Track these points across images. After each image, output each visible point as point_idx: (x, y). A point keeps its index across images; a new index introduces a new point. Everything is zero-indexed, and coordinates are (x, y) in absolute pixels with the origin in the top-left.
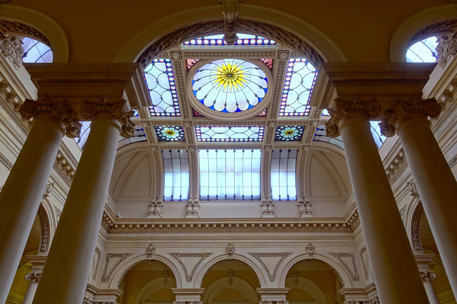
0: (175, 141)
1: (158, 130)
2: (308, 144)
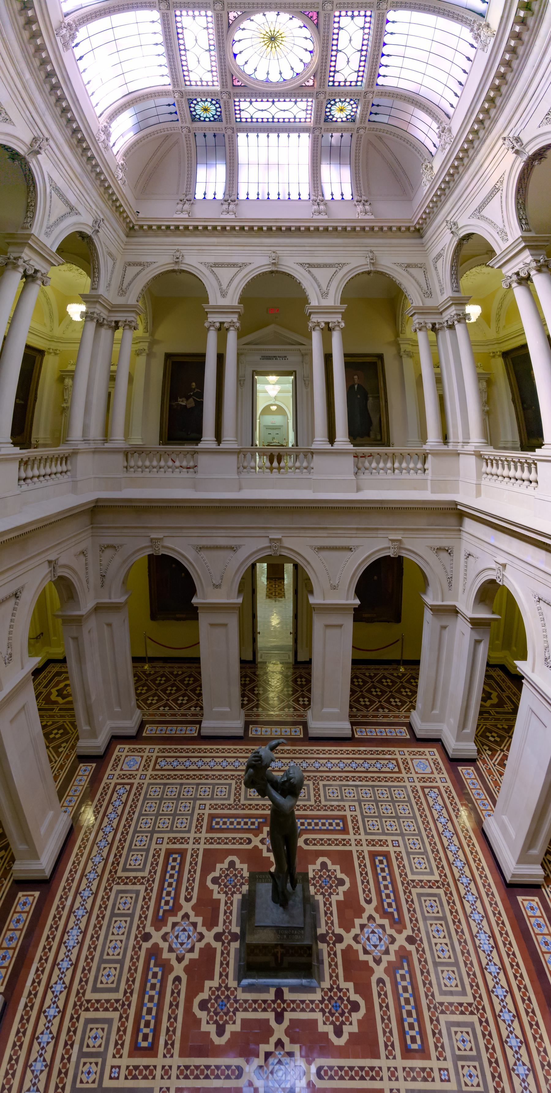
0: (210, 121)
1: (192, 105)
2: (363, 125)
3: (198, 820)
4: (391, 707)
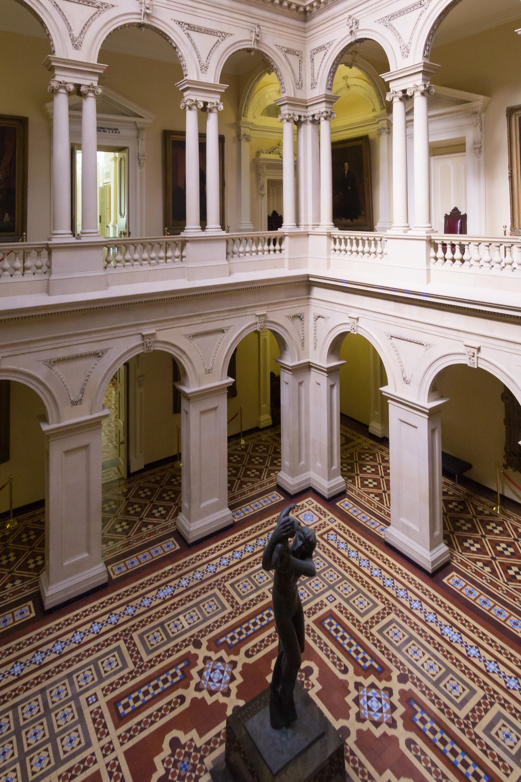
3: (94, 720)
4: (252, 480)
